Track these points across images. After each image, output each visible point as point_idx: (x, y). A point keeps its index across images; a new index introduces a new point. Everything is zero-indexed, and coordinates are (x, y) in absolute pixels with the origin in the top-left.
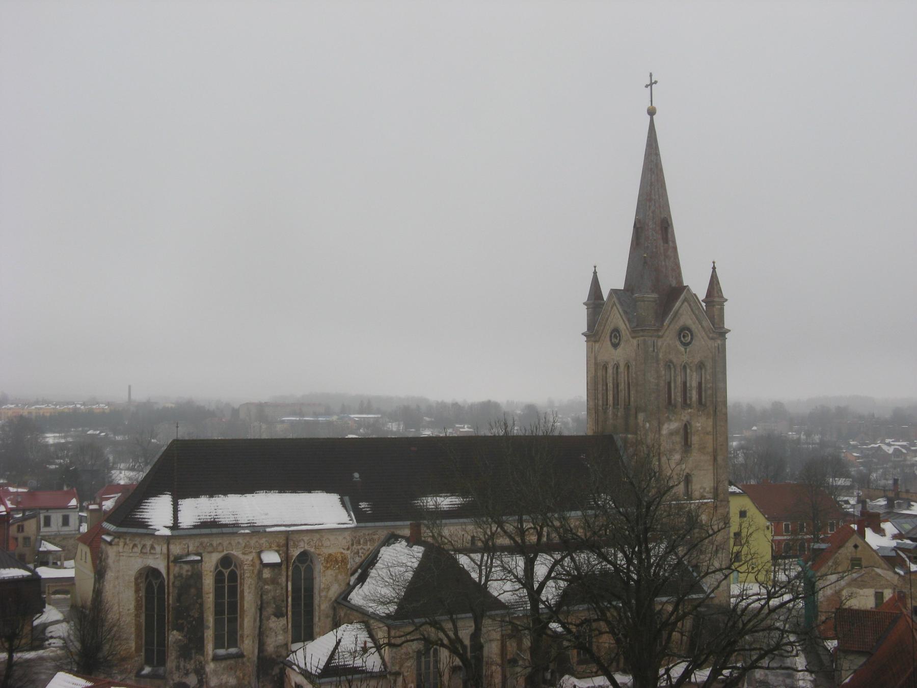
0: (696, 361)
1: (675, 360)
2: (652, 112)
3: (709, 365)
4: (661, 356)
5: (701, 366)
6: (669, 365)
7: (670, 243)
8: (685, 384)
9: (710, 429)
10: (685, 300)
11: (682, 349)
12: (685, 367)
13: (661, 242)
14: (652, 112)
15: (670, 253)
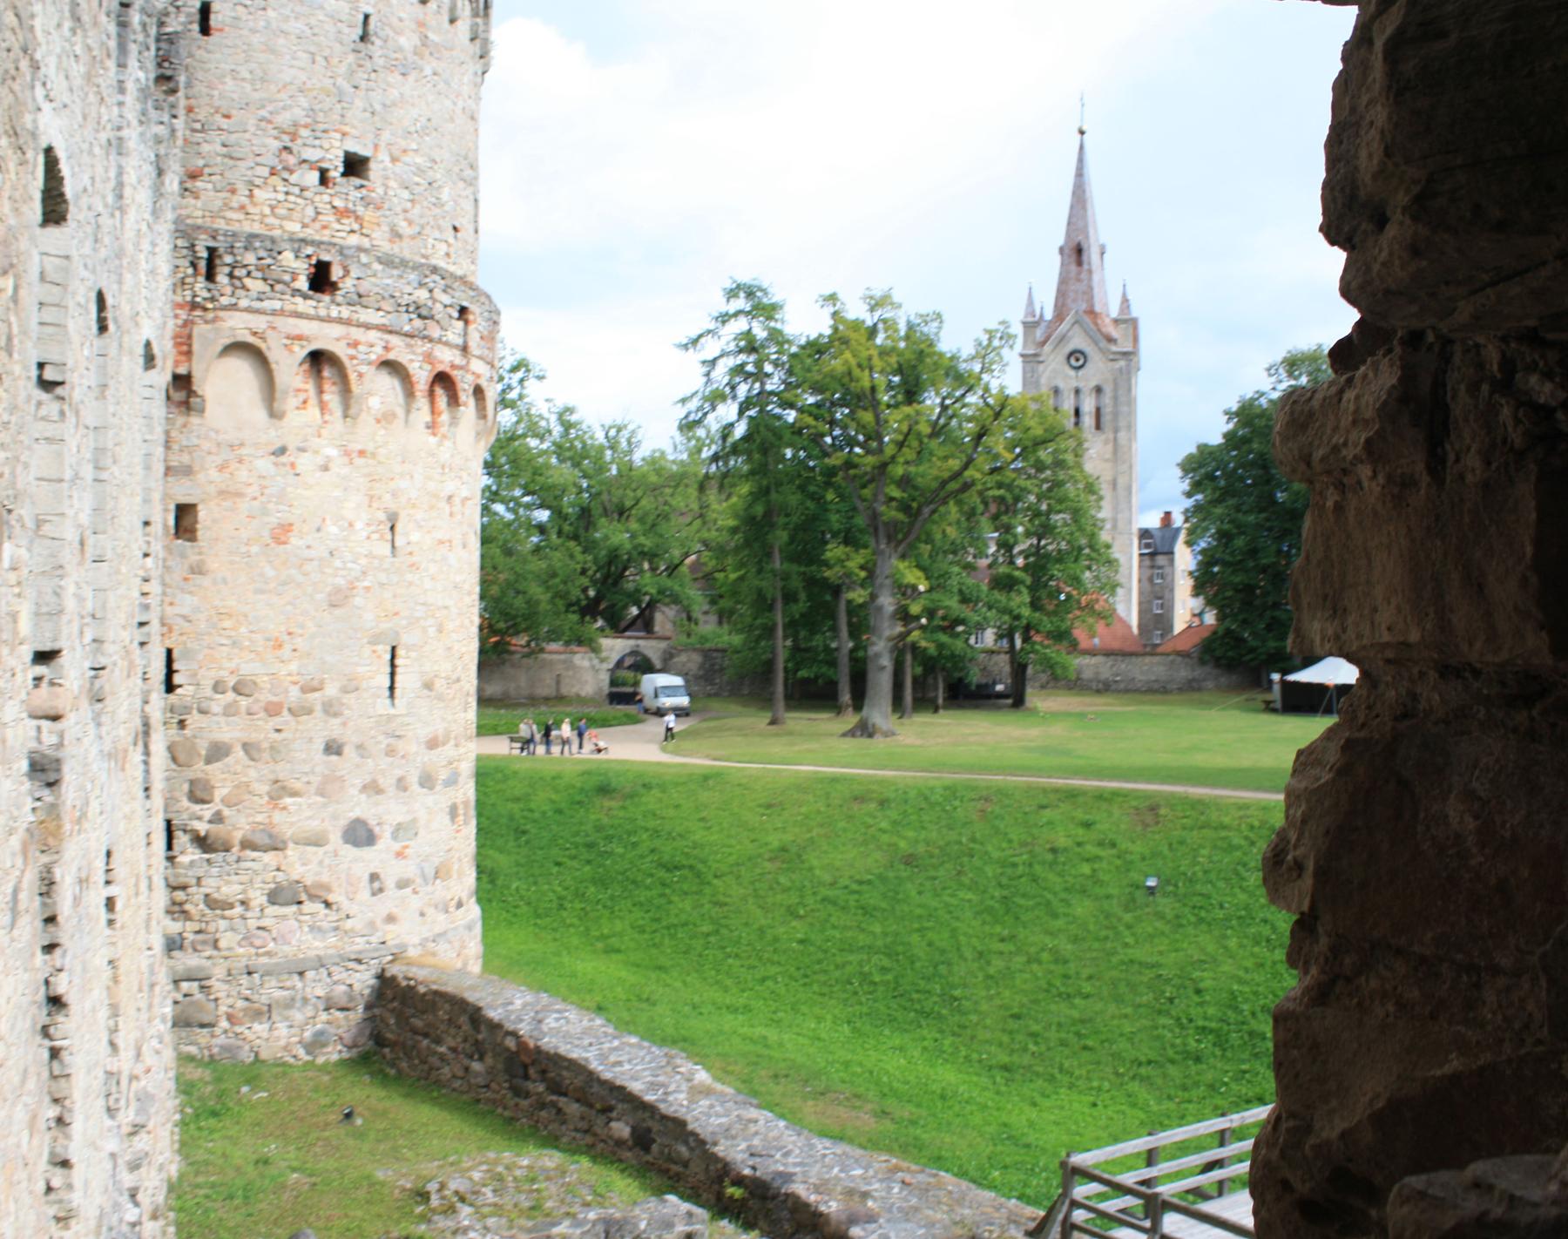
0: (1093, 383)
1: (1061, 385)
2: (1082, 133)
3: (1108, 389)
4: (1043, 381)
5: (1099, 390)
6: (1056, 391)
7: (1086, 267)
8: (1077, 412)
9: (1108, 456)
10: (1076, 322)
11: (1072, 373)
12: (1077, 392)
13: (1073, 268)
14: (1082, 133)
15: (1084, 276)
